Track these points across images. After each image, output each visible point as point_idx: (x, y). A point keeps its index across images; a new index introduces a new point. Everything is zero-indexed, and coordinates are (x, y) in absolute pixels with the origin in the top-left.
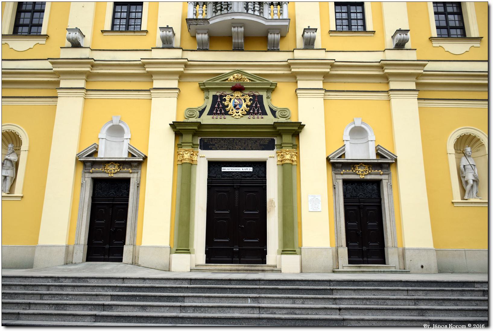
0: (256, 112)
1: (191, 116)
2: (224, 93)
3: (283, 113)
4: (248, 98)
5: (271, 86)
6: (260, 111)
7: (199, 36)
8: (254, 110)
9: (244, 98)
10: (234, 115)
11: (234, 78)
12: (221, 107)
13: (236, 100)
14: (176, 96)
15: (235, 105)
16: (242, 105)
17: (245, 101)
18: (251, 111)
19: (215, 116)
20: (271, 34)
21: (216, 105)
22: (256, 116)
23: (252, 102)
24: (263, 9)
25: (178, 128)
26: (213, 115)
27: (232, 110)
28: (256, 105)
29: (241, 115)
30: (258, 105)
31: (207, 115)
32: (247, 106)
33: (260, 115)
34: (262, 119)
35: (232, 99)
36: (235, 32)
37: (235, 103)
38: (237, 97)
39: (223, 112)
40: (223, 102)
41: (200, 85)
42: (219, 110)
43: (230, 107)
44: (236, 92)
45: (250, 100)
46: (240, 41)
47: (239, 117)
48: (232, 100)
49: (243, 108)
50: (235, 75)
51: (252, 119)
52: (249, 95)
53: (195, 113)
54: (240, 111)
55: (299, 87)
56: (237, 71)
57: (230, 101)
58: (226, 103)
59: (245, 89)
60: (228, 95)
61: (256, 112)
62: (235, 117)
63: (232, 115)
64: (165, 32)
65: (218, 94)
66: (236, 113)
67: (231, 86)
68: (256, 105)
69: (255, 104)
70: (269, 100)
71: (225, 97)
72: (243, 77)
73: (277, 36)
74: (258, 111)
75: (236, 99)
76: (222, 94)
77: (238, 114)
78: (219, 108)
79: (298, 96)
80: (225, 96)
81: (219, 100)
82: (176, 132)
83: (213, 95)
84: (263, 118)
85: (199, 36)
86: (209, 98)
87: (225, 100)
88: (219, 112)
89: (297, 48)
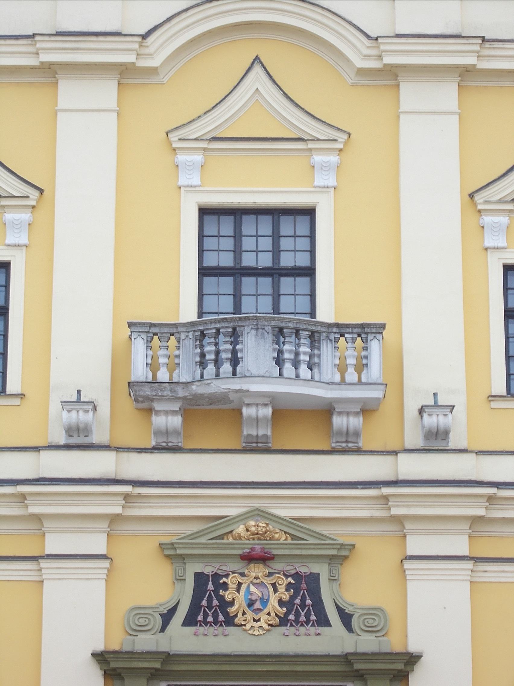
0: (303, 618)
1: (141, 629)
2: (222, 568)
3: (371, 621)
4: (283, 582)
5: (339, 549)
6: (313, 617)
7: (159, 421)
8: (297, 615)
9: (274, 582)
10: (248, 627)
11: (247, 530)
12: (217, 605)
13: (253, 589)
14: (105, 577)
15: (251, 600)
16: (268, 600)
17: (276, 590)
18: (292, 617)
19: (201, 630)
20: (340, 413)
21: (203, 600)
22: (302, 630)
23: (292, 591)
24: (319, 356)
25: (113, 665)
26: (196, 626)
27: (244, 613)
28: (303, 600)
29: (265, 626)
30: (309, 602)
31: (182, 625)
32: (281, 603)
33: (313, 625)
34: (317, 636)
35: (242, 584)
36: (250, 417)
37: (251, 594)
38: (256, 578)
39: (221, 618)
40: (221, 593)
41: (163, 547)
42: (210, 613)
43: (239, 607)
44: (252, 565)
45: (289, 587)
46: (261, 433)
47: (262, 632)
48: (243, 588)
49: (271, 608)
50: (252, 523)
51: (292, 638)
52: (284, 575)
53: (152, 619)
54: (264, 617)
55: (410, 552)
56: (256, 512)
57: (238, 590)
58: (228, 596)
59: (275, 557)
60: (233, 572)
61: (303, 618)
62: (250, 632)
63: (245, 625)
64: (74, 414)
65: (208, 570)
66: (255, 620)
67: (240, 552)
68: (303, 600)
69: (299, 597)
70: (335, 585)
71: (224, 579)
72: (271, 527)
73: (355, 422)
74: (308, 615)
75: (254, 584)
76: (219, 572)
77: (259, 624)
78: (210, 607)
79: (408, 578)
80: (227, 576)
81: (210, 586)
82: (106, 672)
83: (195, 573)
84: (319, 634)
85: (159, 421)
86: (185, 580)
87: (225, 587)
88: (210, 619)
89: (408, 446)
